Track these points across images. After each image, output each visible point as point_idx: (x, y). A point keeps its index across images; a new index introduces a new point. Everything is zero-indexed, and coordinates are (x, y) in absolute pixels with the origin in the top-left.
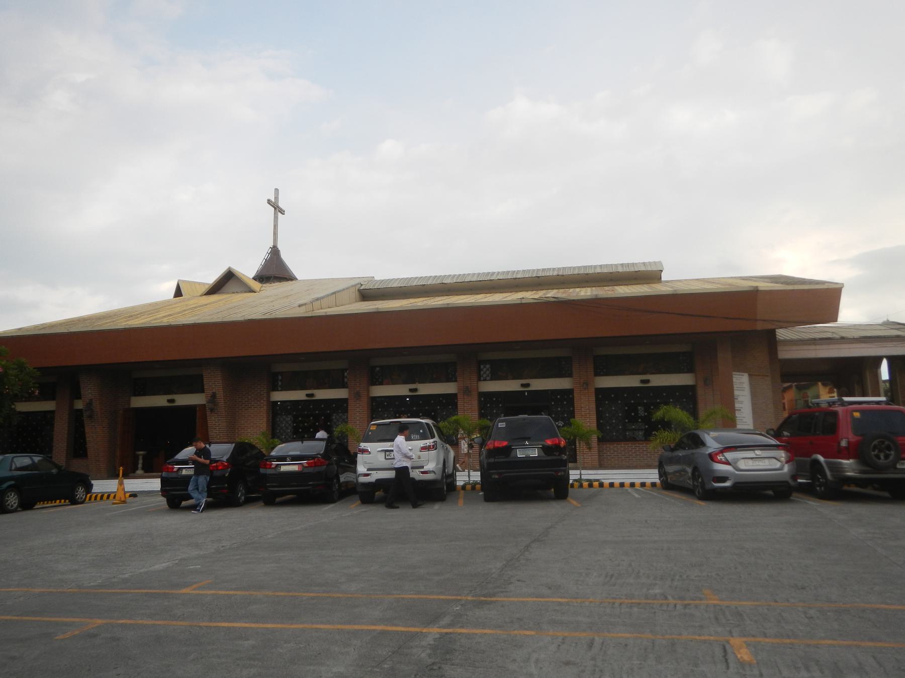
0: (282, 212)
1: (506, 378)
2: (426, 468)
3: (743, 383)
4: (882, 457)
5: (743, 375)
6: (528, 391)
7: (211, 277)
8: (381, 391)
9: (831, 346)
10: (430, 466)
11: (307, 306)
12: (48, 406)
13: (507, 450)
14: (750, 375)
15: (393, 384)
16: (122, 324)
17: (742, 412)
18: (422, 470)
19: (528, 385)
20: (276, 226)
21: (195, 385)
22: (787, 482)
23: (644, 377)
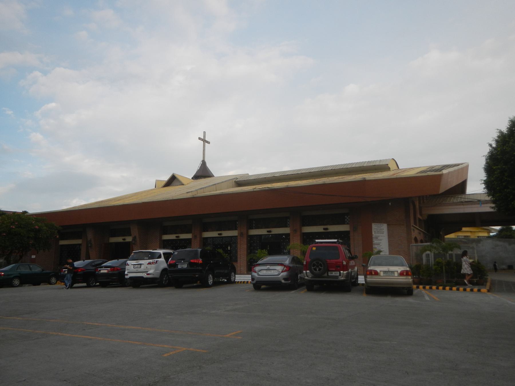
0: (209, 143)
1: (261, 228)
2: (149, 272)
3: (383, 229)
4: (318, 270)
5: (383, 225)
6: (271, 234)
7: (166, 178)
8: (166, 237)
9: (473, 206)
10: (151, 272)
11: (193, 192)
12: (79, 242)
13: (174, 265)
14: (387, 225)
15: (213, 231)
16: (127, 202)
17: (381, 245)
18: (147, 273)
19: (270, 231)
20: (204, 150)
21: (127, 232)
22: (280, 282)
23: (326, 227)
